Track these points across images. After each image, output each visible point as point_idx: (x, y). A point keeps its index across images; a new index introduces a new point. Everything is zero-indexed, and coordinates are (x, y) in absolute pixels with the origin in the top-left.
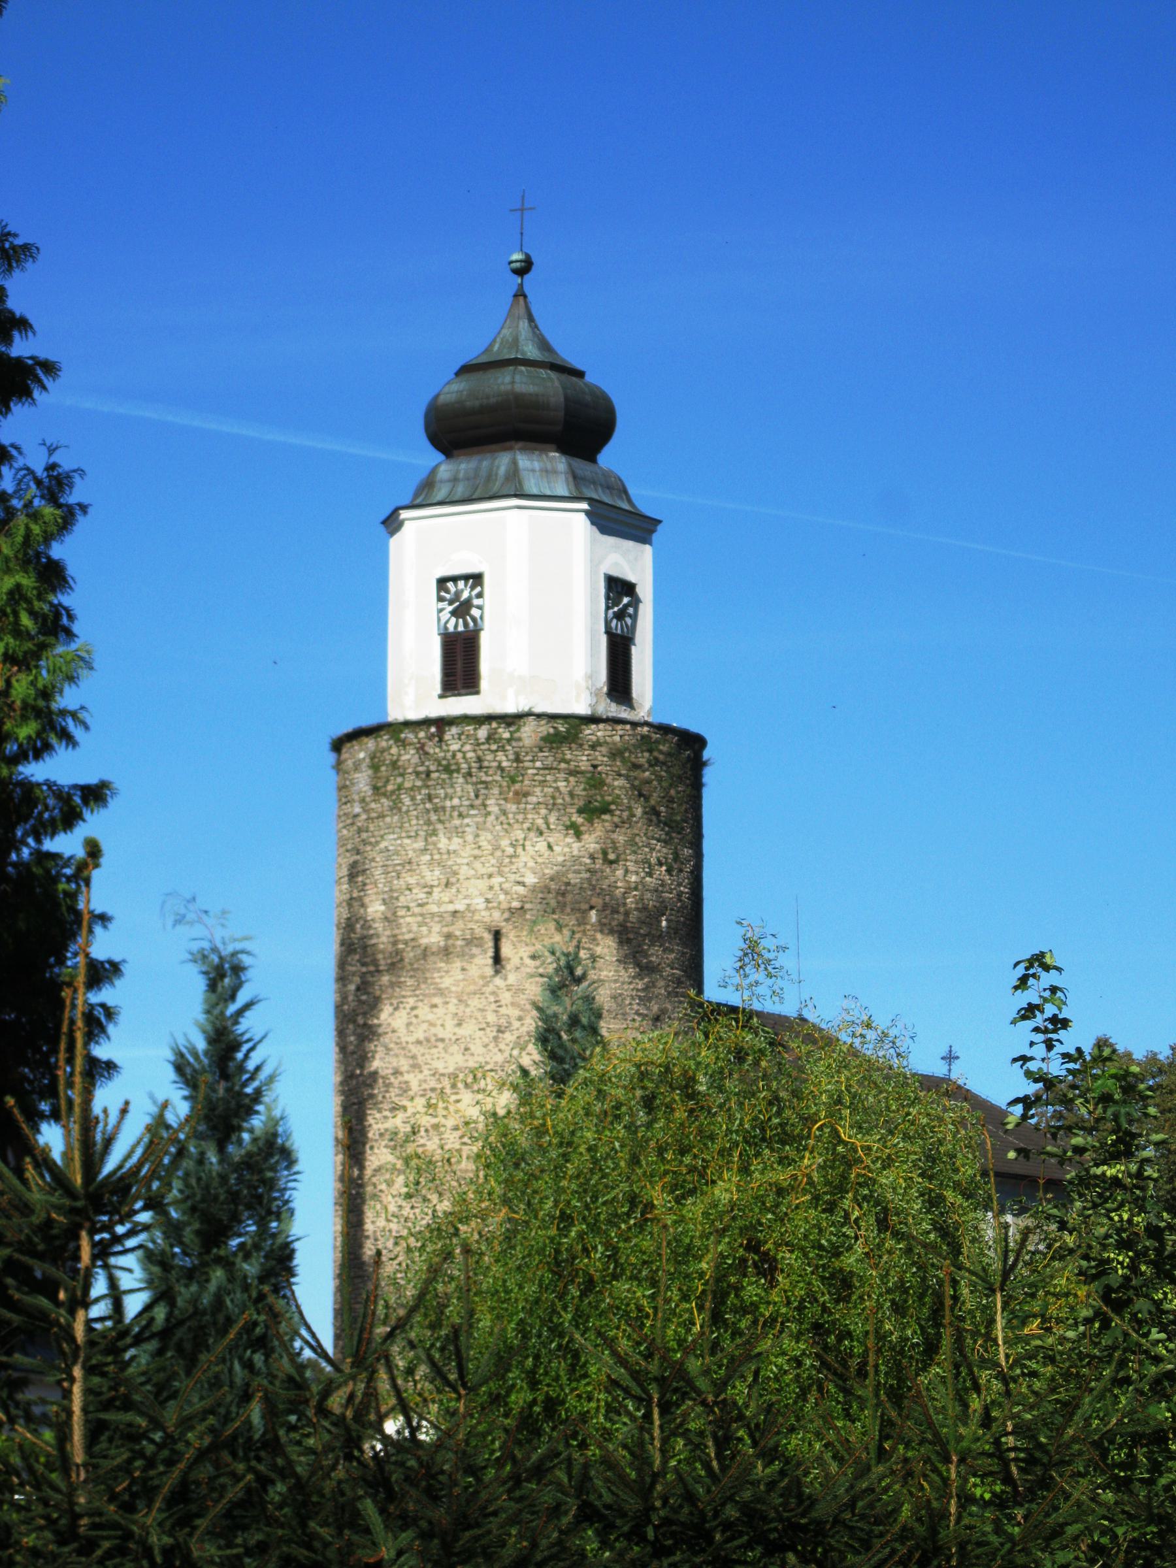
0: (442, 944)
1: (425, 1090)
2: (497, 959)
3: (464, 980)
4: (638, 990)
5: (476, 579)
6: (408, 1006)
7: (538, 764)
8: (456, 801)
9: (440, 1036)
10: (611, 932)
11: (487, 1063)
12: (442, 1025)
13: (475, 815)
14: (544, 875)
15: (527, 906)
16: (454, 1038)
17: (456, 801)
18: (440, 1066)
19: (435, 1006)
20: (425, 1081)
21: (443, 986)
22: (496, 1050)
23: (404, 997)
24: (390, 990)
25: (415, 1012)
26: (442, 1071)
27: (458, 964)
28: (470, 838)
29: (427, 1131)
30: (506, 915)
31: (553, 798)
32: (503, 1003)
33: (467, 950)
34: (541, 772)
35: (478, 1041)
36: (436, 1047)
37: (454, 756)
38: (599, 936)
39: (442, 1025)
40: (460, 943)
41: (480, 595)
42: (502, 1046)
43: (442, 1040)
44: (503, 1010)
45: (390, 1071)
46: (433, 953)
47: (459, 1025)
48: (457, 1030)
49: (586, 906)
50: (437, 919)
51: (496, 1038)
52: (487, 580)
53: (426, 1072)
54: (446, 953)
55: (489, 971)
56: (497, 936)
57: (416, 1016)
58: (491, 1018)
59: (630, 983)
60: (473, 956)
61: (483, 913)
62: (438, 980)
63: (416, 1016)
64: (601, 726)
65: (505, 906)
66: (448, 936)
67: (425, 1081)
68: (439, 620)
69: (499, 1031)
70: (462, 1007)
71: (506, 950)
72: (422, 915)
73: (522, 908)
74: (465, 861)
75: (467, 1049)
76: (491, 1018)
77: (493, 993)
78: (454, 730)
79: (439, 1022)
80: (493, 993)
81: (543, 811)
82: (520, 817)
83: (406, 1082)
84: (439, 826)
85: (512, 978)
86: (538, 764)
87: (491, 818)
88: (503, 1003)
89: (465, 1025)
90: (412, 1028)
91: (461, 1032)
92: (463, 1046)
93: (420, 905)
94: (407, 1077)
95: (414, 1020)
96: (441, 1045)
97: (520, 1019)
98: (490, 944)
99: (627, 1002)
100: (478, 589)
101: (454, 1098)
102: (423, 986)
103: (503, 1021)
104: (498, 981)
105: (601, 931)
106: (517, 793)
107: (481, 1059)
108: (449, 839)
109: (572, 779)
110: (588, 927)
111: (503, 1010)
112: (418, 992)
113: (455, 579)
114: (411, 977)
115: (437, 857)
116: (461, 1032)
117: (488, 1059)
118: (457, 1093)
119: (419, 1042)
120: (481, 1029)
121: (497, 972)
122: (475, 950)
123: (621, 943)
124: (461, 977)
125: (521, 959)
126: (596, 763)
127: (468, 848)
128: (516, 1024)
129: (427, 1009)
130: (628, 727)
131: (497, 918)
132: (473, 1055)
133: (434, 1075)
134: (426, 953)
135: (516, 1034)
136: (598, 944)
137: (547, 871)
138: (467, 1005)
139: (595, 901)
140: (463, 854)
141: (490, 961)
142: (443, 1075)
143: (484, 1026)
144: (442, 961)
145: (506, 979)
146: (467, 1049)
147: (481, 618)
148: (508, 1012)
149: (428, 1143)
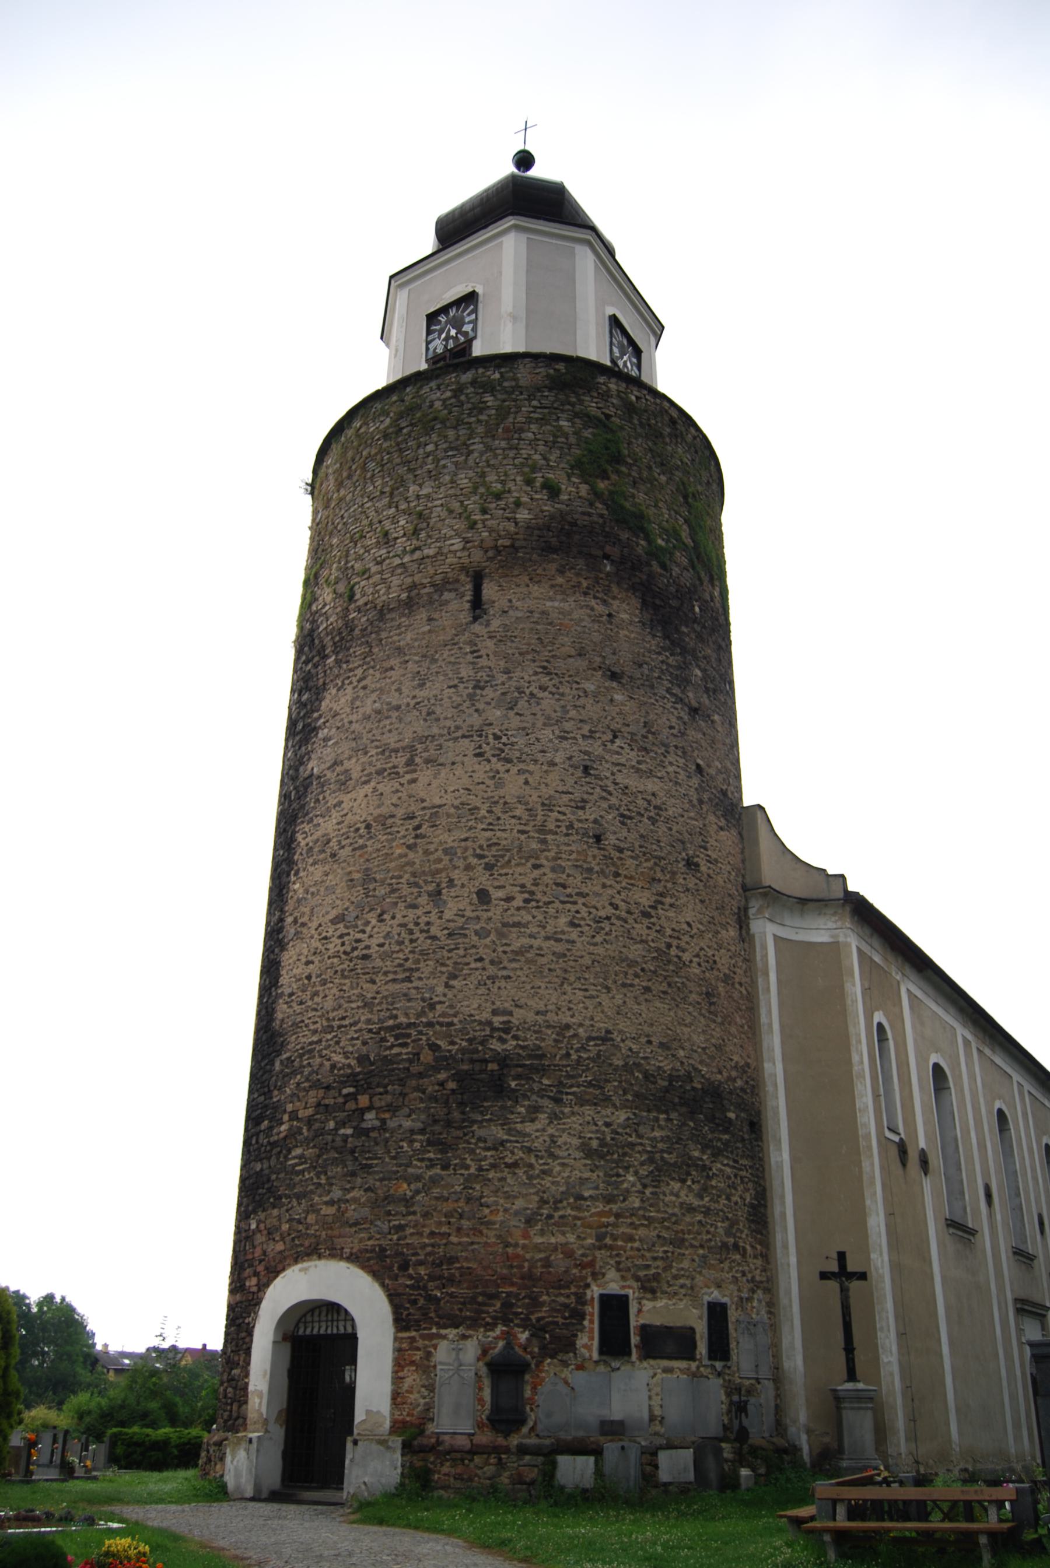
0: (404, 596)
1: (371, 774)
2: (477, 604)
3: (430, 631)
4: (668, 664)
5: (470, 299)
6: (354, 679)
7: (535, 403)
8: (430, 448)
9: (394, 703)
10: (633, 588)
11: (458, 728)
12: (399, 690)
13: (454, 456)
14: (542, 511)
15: (517, 544)
16: (412, 703)
17: (430, 448)
18: (391, 740)
19: (392, 669)
20: (370, 764)
21: (402, 643)
22: (472, 710)
23: (351, 670)
24: (336, 671)
25: (362, 684)
26: (393, 746)
27: (422, 615)
28: (447, 478)
29: (368, 827)
30: (490, 554)
31: (555, 436)
32: (483, 652)
33: (436, 597)
34: (539, 410)
35: (446, 702)
36: (387, 718)
37: (431, 407)
38: (615, 589)
39: (399, 690)
40: (426, 590)
41: (475, 311)
42: (481, 706)
43: (398, 708)
44: (483, 662)
45: (328, 765)
46: (391, 610)
47: (422, 685)
48: (417, 692)
49: (600, 553)
50: (399, 571)
51: (471, 697)
52: (481, 299)
53: (373, 752)
54: (409, 605)
55: (465, 617)
56: (478, 579)
57: (364, 688)
58: (465, 672)
59: (659, 653)
60: (447, 602)
61: (459, 554)
62: (396, 638)
63: (364, 688)
64: (613, 380)
65: (492, 544)
66: (414, 586)
67: (370, 764)
68: (427, 349)
69: (475, 687)
70: (426, 664)
71: (489, 590)
72: (379, 573)
73: (512, 546)
74: (439, 502)
75: (429, 714)
76: (465, 672)
77: (472, 643)
78: (433, 384)
79: (393, 688)
80: (472, 643)
81: (541, 448)
82: (512, 454)
83: (346, 771)
84: (410, 476)
85: (495, 624)
86: (535, 403)
87: (476, 455)
88: (483, 652)
89: (428, 685)
90: (358, 703)
91: (421, 694)
92: (424, 711)
93: (378, 563)
94: (347, 765)
95: (361, 693)
96: (396, 714)
97: (507, 672)
98: (469, 586)
99: (656, 675)
100: (472, 307)
101: (408, 777)
102: (375, 650)
103: (483, 675)
104: (477, 628)
105: (618, 584)
106: (506, 430)
107: (448, 723)
108: (420, 485)
109: (577, 421)
110: (602, 575)
111: (483, 662)
112: (368, 659)
113: (444, 310)
114: (360, 645)
115: (403, 506)
116: (421, 694)
117: (459, 722)
118: (415, 771)
119: (367, 718)
120: (450, 687)
121: (475, 619)
122: (447, 596)
123: (644, 603)
124: (428, 628)
125: (510, 601)
126: (607, 412)
127: (442, 489)
128: (501, 678)
129: (378, 675)
130: (645, 392)
131: (478, 556)
132: (438, 720)
133: (383, 752)
134: (382, 612)
135: (501, 690)
136: (614, 598)
137: (546, 508)
138: (434, 661)
139: (608, 549)
140: (435, 496)
141: (467, 606)
142: (396, 751)
143: (456, 682)
144: (403, 615)
145: (487, 625)
146: (429, 714)
147: (474, 329)
148: (490, 664)
149: (368, 843)
